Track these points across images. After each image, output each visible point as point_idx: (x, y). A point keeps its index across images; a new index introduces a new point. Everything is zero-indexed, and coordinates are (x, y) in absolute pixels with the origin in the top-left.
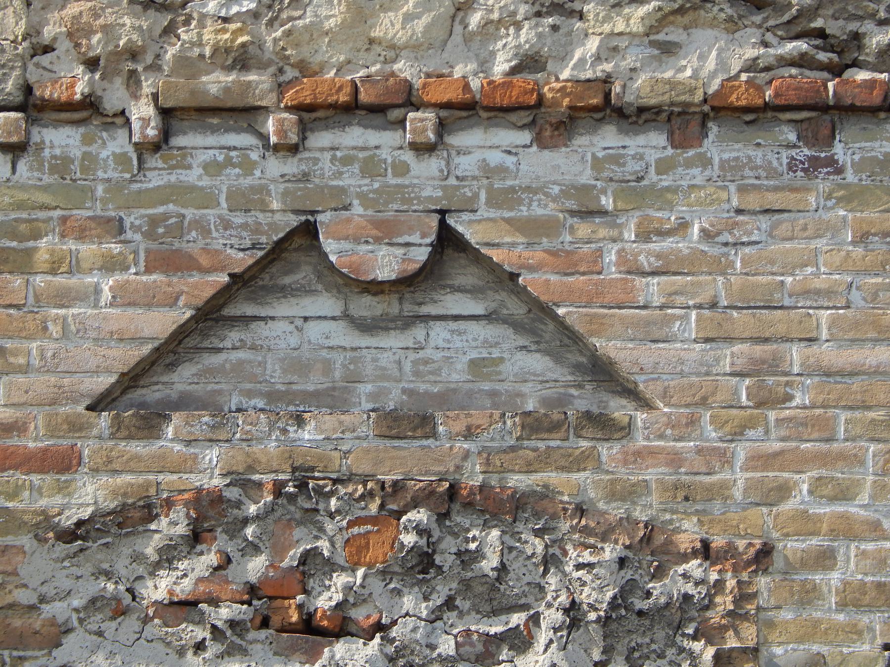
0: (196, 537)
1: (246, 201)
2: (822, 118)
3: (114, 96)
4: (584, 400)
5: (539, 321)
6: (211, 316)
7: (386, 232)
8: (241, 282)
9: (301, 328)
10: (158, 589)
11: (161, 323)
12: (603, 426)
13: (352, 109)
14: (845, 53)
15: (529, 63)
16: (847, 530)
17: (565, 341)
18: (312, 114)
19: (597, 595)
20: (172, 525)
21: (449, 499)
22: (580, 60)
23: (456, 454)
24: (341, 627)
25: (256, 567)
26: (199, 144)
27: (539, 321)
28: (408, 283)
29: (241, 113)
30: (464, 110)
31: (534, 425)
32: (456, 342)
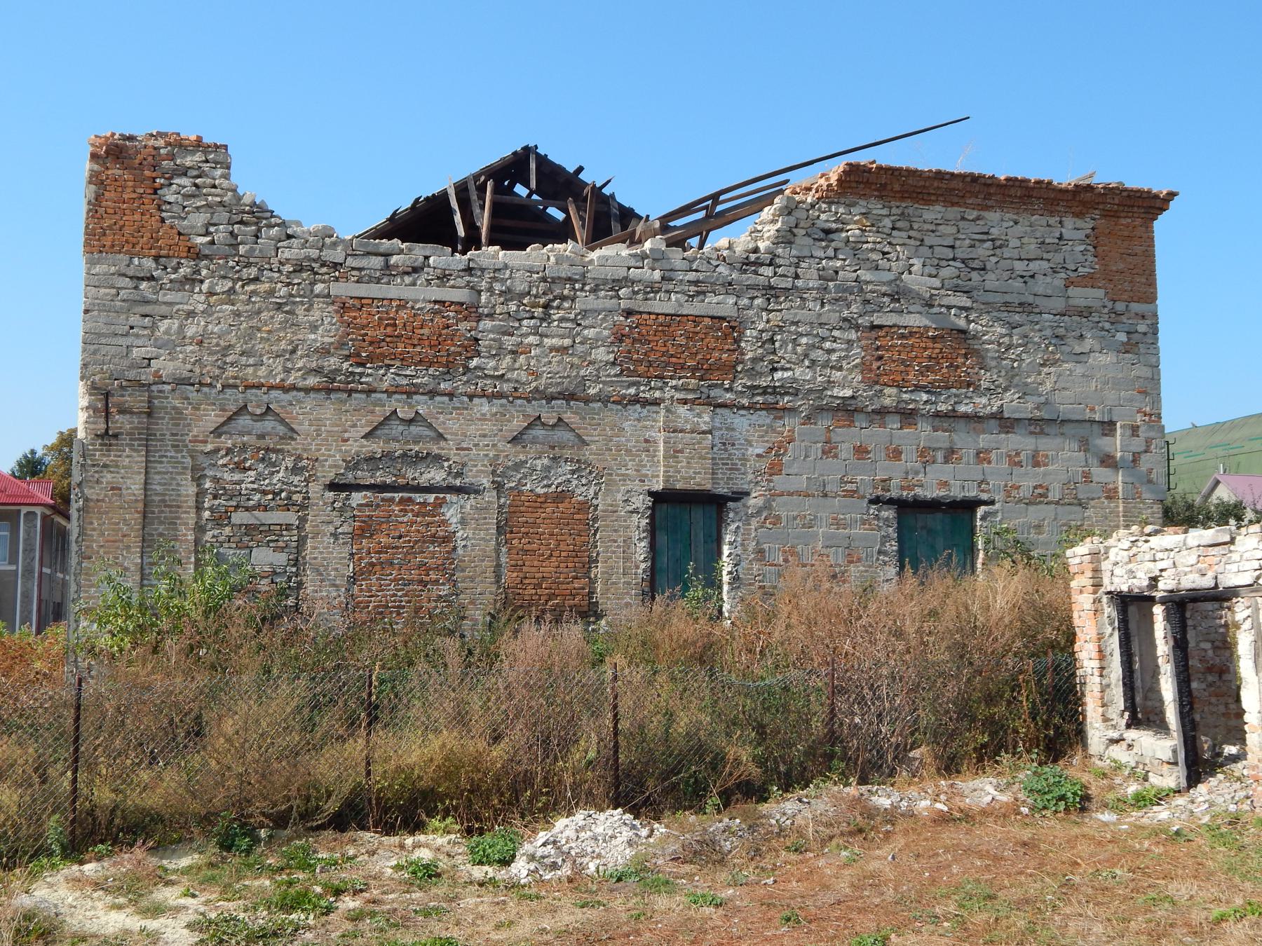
0: (227, 454)
1: (236, 401)
2: (329, 391)
3: (214, 383)
4: (289, 434)
5: (282, 421)
6: (230, 419)
7: (258, 406)
8: (235, 414)
9: (244, 421)
10: (220, 462)
11: (222, 420)
12: (292, 439)
13: (253, 387)
14: (334, 380)
15: (283, 380)
16: (330, 456)
17: (287, 425)
18: (247, 387)
19: (290, 465)
20: (223, 452)
21: (267, 450)
22: (291, 380)
23: (269, 442)
24: (250, 469)
25: (236, 459)
26: (229, 391)
27: (282, 421)
28: (262, 415)
29: (236, 387)
30: (271, 388)
31: (281, 438)
32: (269, 424)
